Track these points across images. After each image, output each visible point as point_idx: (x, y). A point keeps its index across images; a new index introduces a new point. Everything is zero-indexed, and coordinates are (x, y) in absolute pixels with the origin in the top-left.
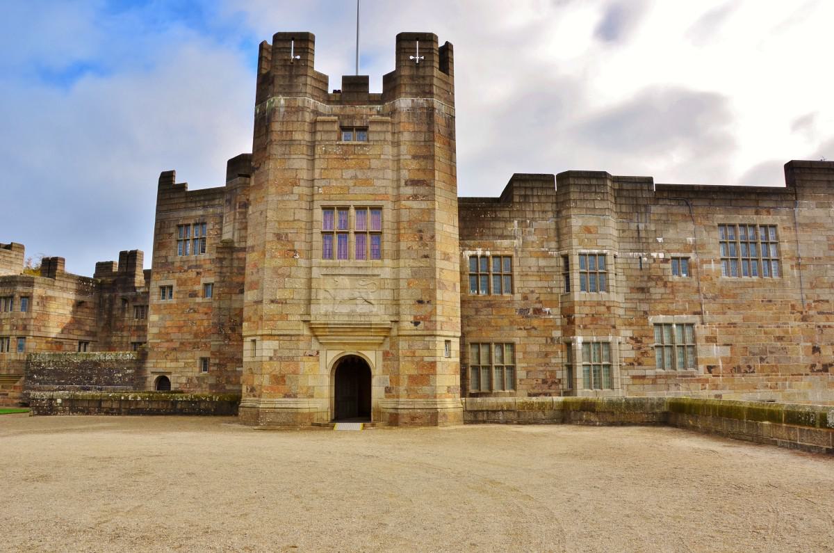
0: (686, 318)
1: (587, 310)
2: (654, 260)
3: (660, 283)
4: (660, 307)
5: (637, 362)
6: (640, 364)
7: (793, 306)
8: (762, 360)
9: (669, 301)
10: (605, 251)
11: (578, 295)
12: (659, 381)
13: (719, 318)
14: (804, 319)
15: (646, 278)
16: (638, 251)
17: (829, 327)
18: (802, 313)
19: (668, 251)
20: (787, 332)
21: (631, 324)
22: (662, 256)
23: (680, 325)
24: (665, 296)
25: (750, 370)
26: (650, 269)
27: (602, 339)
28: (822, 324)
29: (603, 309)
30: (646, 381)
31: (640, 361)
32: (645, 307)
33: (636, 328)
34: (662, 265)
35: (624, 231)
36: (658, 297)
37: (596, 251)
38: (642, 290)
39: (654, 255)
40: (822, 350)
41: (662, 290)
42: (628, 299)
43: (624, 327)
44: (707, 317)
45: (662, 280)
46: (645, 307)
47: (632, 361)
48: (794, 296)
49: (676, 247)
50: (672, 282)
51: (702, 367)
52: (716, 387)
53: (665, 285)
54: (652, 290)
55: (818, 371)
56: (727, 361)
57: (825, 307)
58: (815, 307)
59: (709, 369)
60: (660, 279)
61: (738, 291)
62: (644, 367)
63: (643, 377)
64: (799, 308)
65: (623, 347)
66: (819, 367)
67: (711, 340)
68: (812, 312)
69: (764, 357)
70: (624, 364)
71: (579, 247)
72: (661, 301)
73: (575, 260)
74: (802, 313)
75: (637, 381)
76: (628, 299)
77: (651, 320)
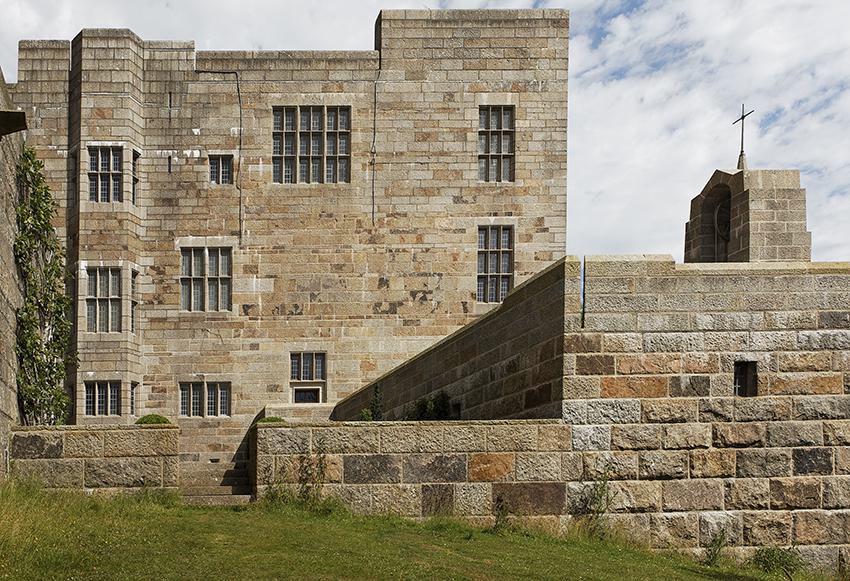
0: (221, 241)
1: (94, 225)
2: (187, 159)
3: (192, 193)
4: (189, 225)
5: (157, 300)
6: (160, 303)
7: (359, 222)
8: (313, 296)
9: (202, 217)
10: (120, 144)
11: (85, 204)
12: (183, 325)
13: (263, 241)
14: (372, 241)
15: (175, 186)
16: (167, 147)
17: (404, 250)
18: (370, 232)
19: (206, 147)
20: (348, 259)
21: (152, 250)
22: (197, 154)
23: (213, 251)
24: (197, 210)
25: (297, 310)
26: (181, 172)
27: (110, 264)
28: (394, 247)
29: (114, 223)
30: (167, 325)
31: (161, 298)
32: (170, 225)
33: (158, 253)
34: (197, 168)
35: (152, 120)
36: (188, 211)
37: (110, 144)
38: (169, 202)
39: (188, 153)
40: (391, 284)
41: (194, 202)
42: (151, 215)
43: (144, 253)
44: (247, 239)
45: (195, 187)
46: (170, 225)
47: (151, 298)
48: (362, 207)
49: (217, 141)
50: (207, 190)
51: (236, 306)
52: (252, 333)
53: (198, 195)
54: (182, 202)
55: (383, 312)
56: (269, 298)
57: (401, 223)
58: (388, 223)
59: (246, 308)
60: (192, 187)
61: (290, 202)
62: (167, 307)
63: (164, 320)
64: (367, 225)
65: (140, 279)
66: (385, 306)
67: (251, 269)
68: (383, 231)
69: (316, 293)
70: (142, 303)
71: (89, 138)
72: (193, 216)
73: (85, 156)
74: (370, 232)
75: (156, 325)
76: (151, 215)
77: (179, 243)
